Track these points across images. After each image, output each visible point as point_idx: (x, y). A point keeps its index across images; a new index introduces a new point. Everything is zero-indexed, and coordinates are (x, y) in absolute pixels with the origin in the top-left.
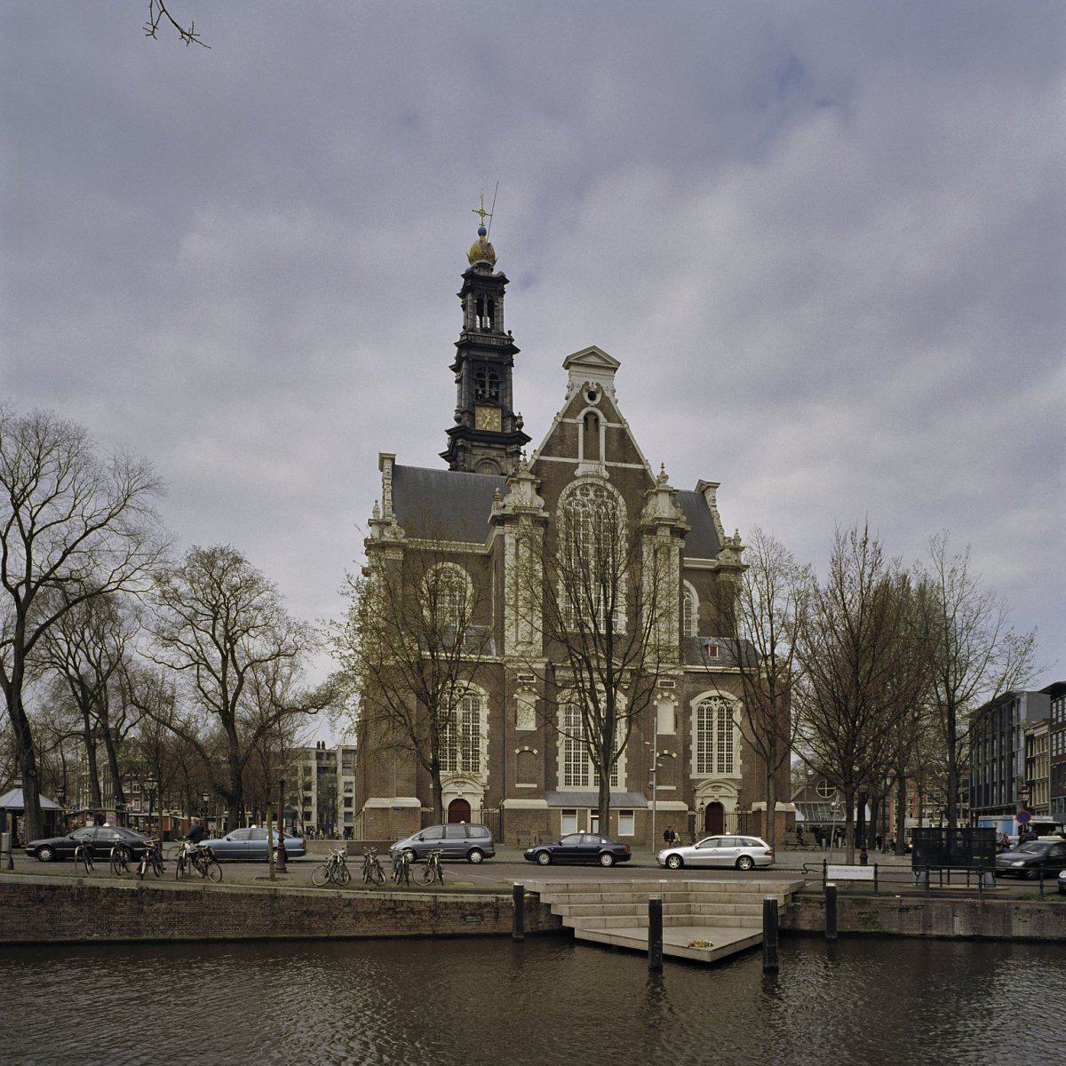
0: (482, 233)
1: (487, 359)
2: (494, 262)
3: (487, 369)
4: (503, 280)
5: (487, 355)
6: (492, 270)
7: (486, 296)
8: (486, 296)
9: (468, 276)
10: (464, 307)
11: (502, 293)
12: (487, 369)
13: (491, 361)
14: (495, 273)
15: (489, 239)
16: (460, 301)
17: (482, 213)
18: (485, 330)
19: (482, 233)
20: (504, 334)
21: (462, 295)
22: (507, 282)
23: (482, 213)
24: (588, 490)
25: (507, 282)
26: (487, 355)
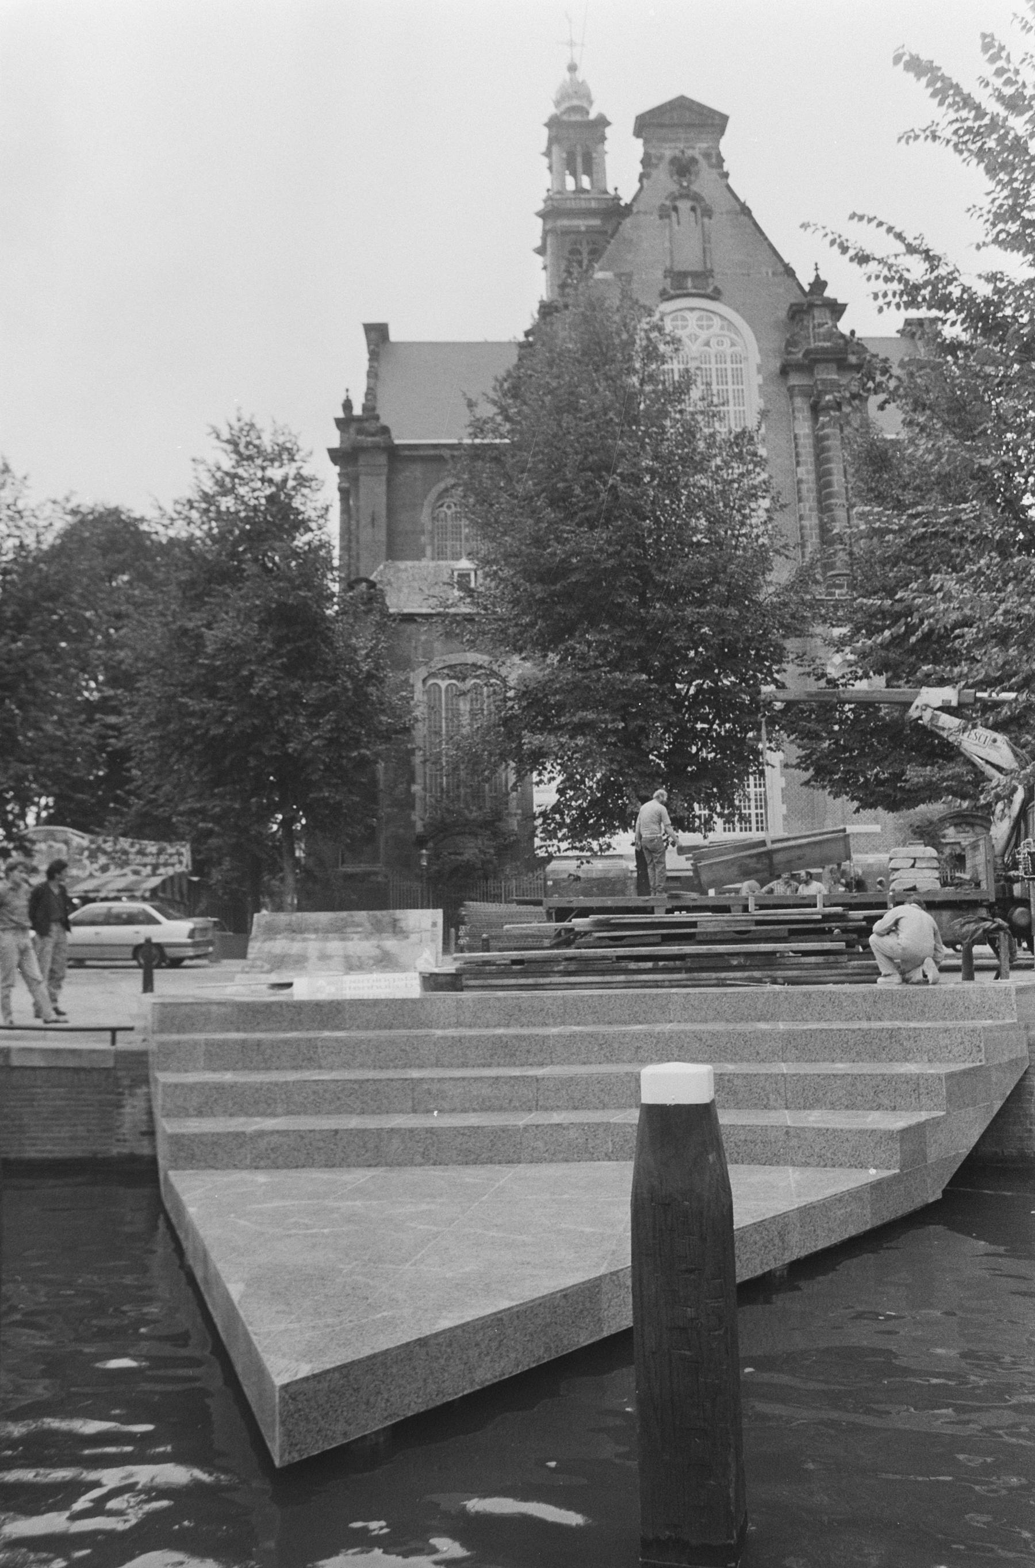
0: (572, 68)
1: (583, 229)
2: (591, 103)
3: (584, 243)
4: (602, 122)
5: (582, 224)
6: (588, 113)
7: (579, 148)
8: (579, 148)
9: (553, 123)
10: (550, 168)
11: (603, 139)
12: (584, 243)
13: (590, 230)
14: (593, 115)
15: (580, 76)
16: (545, 161)
17: (571, 44)
18: (580, 190)
19: (572, 68)
20: (606, 192)
21: (548, 154)
22: (608, 124)
23: (571, 44)
24: (684, 319)
25: (608, 124)
26: (582, 224)
